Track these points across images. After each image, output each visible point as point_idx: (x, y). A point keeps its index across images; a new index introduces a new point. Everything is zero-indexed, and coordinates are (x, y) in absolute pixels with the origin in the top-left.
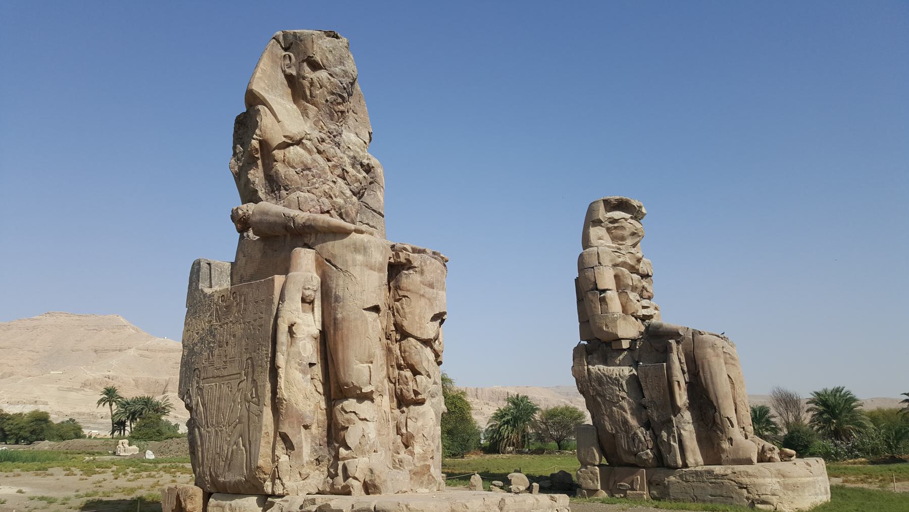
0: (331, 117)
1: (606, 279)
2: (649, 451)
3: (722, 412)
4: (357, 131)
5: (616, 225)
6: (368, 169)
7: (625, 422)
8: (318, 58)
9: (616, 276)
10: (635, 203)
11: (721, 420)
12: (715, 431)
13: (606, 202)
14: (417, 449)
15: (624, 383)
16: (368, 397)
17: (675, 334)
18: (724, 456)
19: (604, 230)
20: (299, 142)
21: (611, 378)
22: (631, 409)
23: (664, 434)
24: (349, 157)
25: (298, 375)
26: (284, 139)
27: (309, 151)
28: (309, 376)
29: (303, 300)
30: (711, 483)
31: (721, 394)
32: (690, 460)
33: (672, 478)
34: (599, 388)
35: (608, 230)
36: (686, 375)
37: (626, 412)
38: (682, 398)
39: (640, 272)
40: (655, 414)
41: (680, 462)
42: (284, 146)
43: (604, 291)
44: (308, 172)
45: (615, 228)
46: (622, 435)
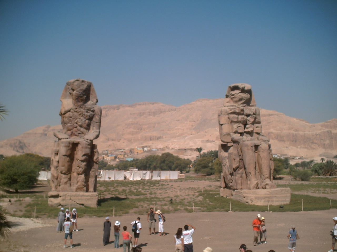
5: (233, 97)
6: (93, 111)
9: (229, 118)
10: (241, 85)
14: (79, 184)
20: (69, 111)
27: (72, 112)
35: (232, 98)
39: (245, 113)
42: (65, 114)
43: (222, 125)
44: (71, 118)
45: (234, 98)
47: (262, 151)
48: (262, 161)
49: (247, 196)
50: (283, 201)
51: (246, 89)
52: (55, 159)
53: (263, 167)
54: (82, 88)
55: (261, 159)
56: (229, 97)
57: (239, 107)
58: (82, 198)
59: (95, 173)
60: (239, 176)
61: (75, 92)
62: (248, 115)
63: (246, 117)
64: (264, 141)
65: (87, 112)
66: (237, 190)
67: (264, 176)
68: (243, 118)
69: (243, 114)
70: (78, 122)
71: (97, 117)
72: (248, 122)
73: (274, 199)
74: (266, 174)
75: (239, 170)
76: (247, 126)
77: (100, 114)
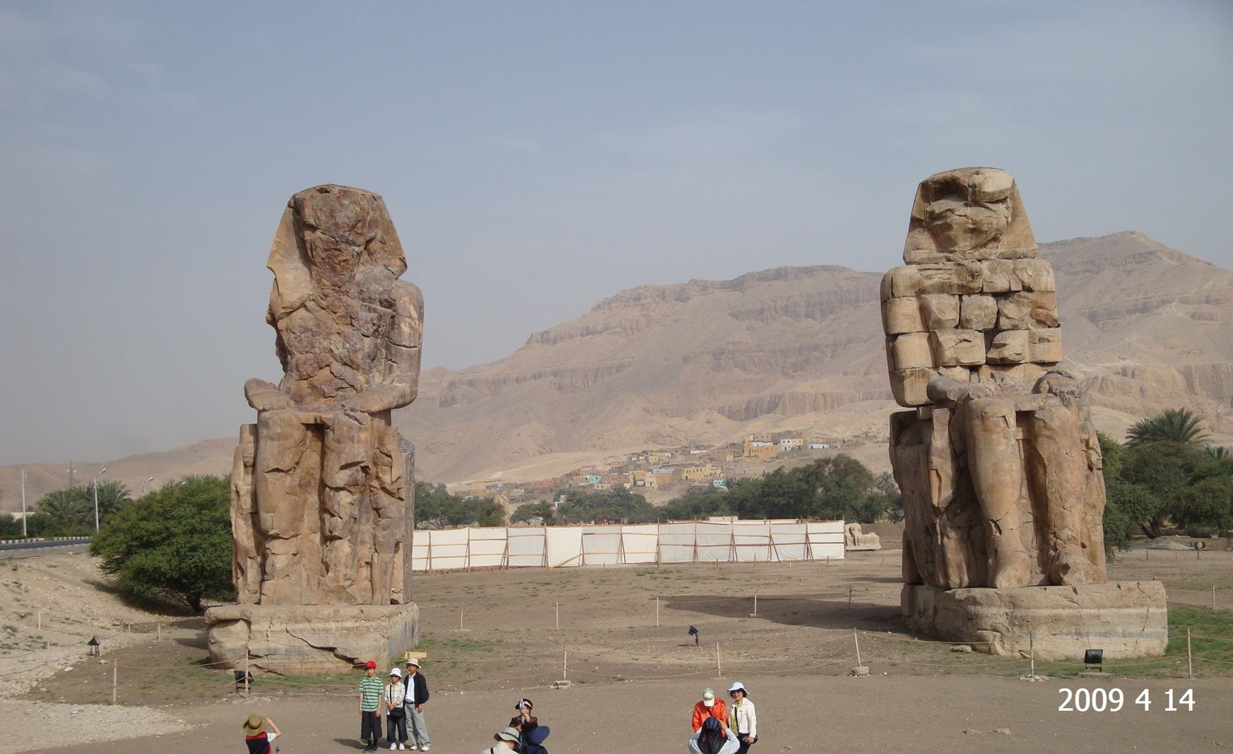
0: (333, 269)
4: (386, 262)
8: (312, 221)
13: (924, 186)
14: (331, 574)
16: (276, 537)
24: (363, 300)
25: (241, 522)
26: (283, 311)
28: (250, 522)
29: (245, 466)
31: (984, 486)
32: (954, 579)
38: (942, 492)
39: (985, 290)
41: (942, 581)
43: (895, 336)
47: (1048, 433)
48: (1045, 473)
49: (977, 615)
50: (1131, 635)
51: (989, 188)
52: (243, 483)
54: (342, 218)
55: (1045, 468)
58: (333, 625)
59: (393, 535)
61: (318, 233)
65: (370, 310)
69: (982, 293)
70: (333, 348)
71: (402, 325)
72: (1004, 322)
76: (999, 339)
77: (415, 314)
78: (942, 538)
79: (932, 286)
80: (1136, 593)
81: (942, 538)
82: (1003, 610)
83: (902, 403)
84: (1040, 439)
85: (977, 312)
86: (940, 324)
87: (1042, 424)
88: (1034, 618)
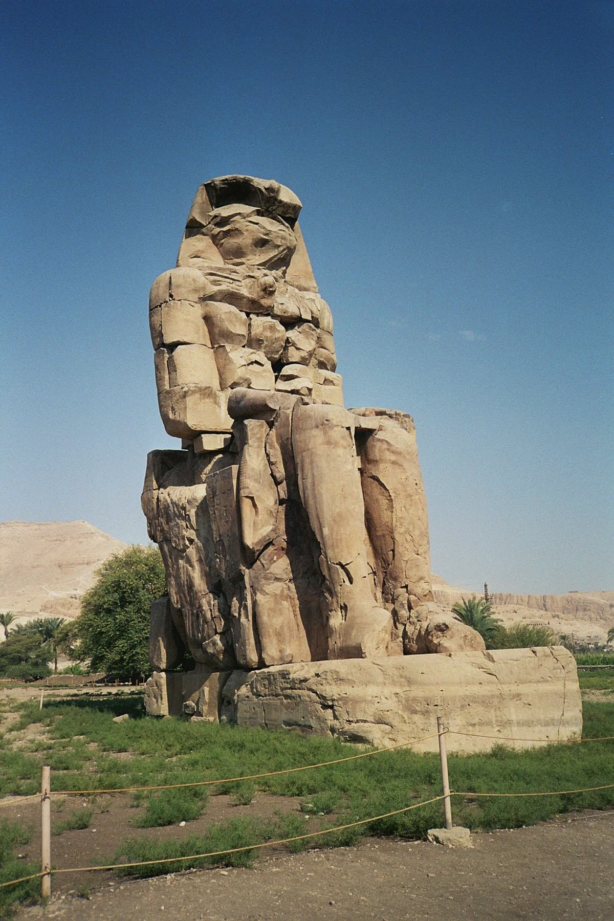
1: (184, 322)
2: (217, 638)
3: (330, 553)
5: (225, 229)
7: (191, 585)
9: (207, 319)
11: (329, 568)
12: (323, 592)
15: (192, 512)
17: (261, 411)
18: (331, 642)
19: (207, 240)
21: (177, 506)
22: (200, 560)
23: (235, 602)
30: (287, 697)
33: (244, 690)
34: (166, 528)
35: (214, 238)
36: (283, 488)
37: (192, 566)
39: (277, 311)
40: (223, 567)
41: (253, 657)
45: (227, 234)
46: (187, 610)
47: (393, 458)
49: (345, 700)
53: (397, 537)
55: (391, 500)
56: (204, 230)
57: (251, 274)
60: (279, 592)
62: (290, 322)
63: (282, 328)
64: (390, 416)
66: (266, 670)
67: (406, 587)
68: (272, 328)
73: (513, 712)
74: (421, 578)
75: (272, 561)
76: (287, 370)
78: (254, 593)
79: (220, 292)
80: (551, 660)
81: (254, 593)
82: (388, 690)
83: (174, 428)
84: (382, 466)
85: (268, 334)
86: (229, 336)
87: (385, 446)
88: (444, 699)
